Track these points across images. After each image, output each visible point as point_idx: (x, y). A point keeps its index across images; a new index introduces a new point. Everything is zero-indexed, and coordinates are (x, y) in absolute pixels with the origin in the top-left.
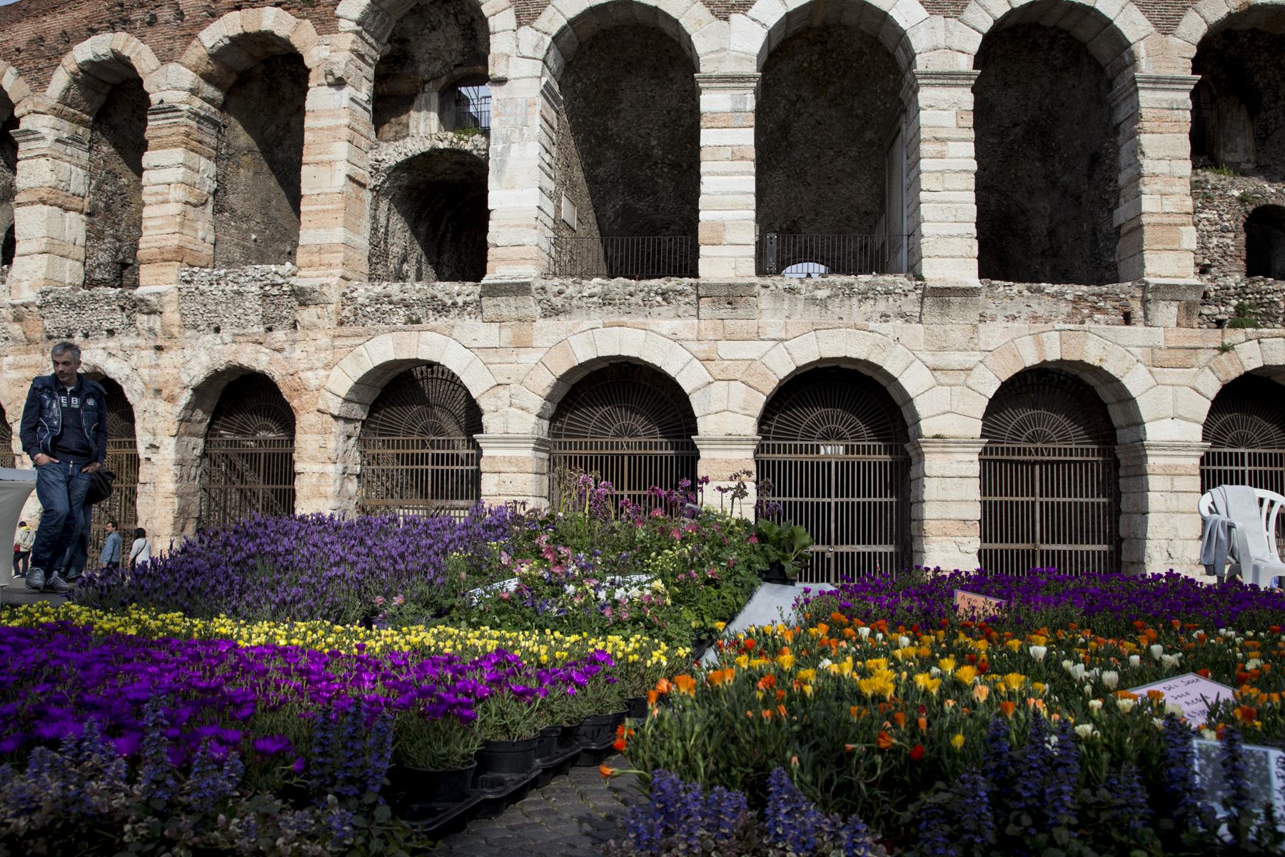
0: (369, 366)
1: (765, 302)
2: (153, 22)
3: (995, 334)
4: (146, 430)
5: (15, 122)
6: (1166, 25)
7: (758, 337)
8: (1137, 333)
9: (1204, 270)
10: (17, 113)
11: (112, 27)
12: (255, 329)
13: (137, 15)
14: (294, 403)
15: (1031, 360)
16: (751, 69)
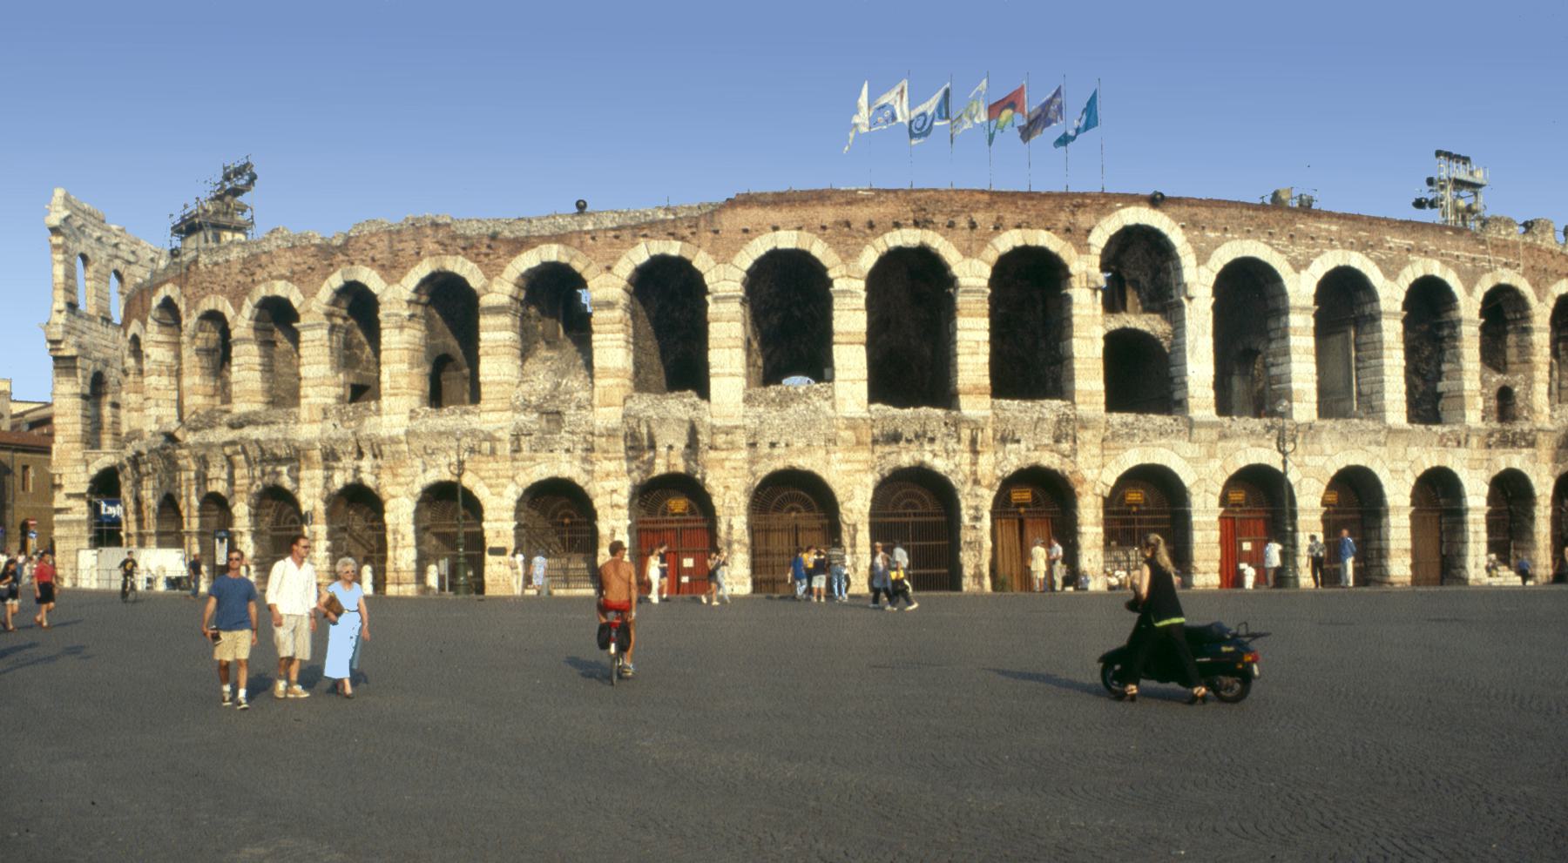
0: (1126, 468)
1: (1324, 435)
2: (951, 225)
3: (1414, 451)
4: (970, 507)
5: (830, 283)
6: (1470, 290)
7: (1322, 453)
8: (1462, 451)
9: (1483, 418)
10: (831, 274)
11: (916, 224)
12: (1046, 441)
13: (939, 219)
14: (1078, 489)
15: (1428, 466)
16: (1310, 302)
